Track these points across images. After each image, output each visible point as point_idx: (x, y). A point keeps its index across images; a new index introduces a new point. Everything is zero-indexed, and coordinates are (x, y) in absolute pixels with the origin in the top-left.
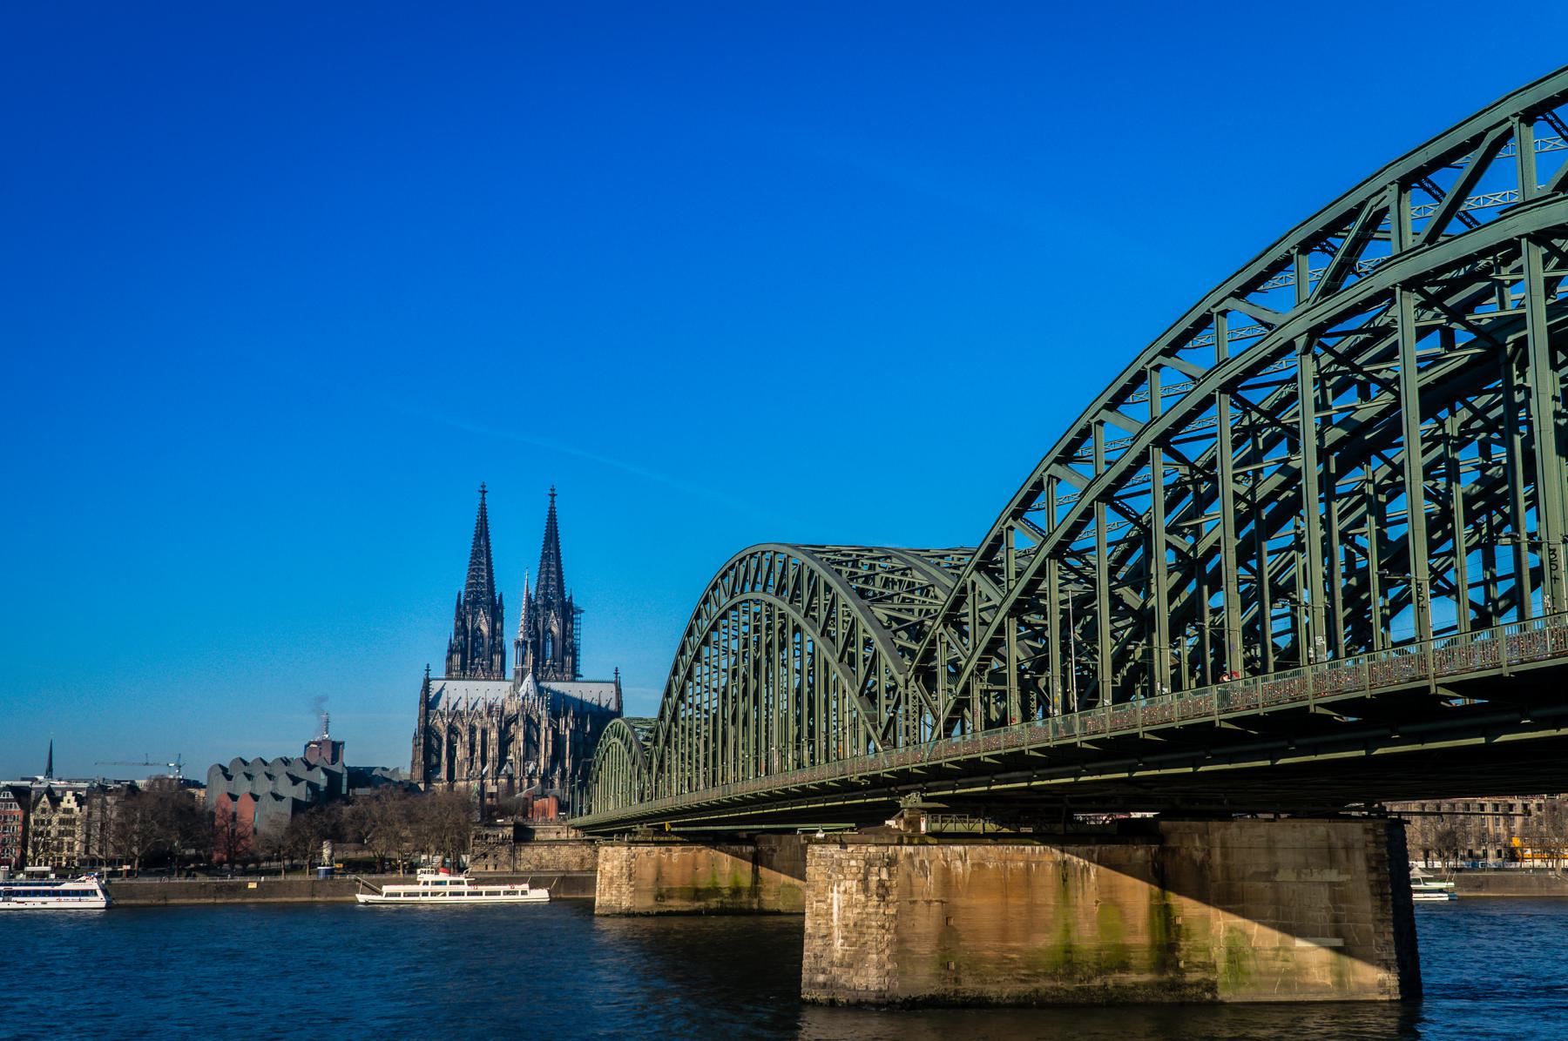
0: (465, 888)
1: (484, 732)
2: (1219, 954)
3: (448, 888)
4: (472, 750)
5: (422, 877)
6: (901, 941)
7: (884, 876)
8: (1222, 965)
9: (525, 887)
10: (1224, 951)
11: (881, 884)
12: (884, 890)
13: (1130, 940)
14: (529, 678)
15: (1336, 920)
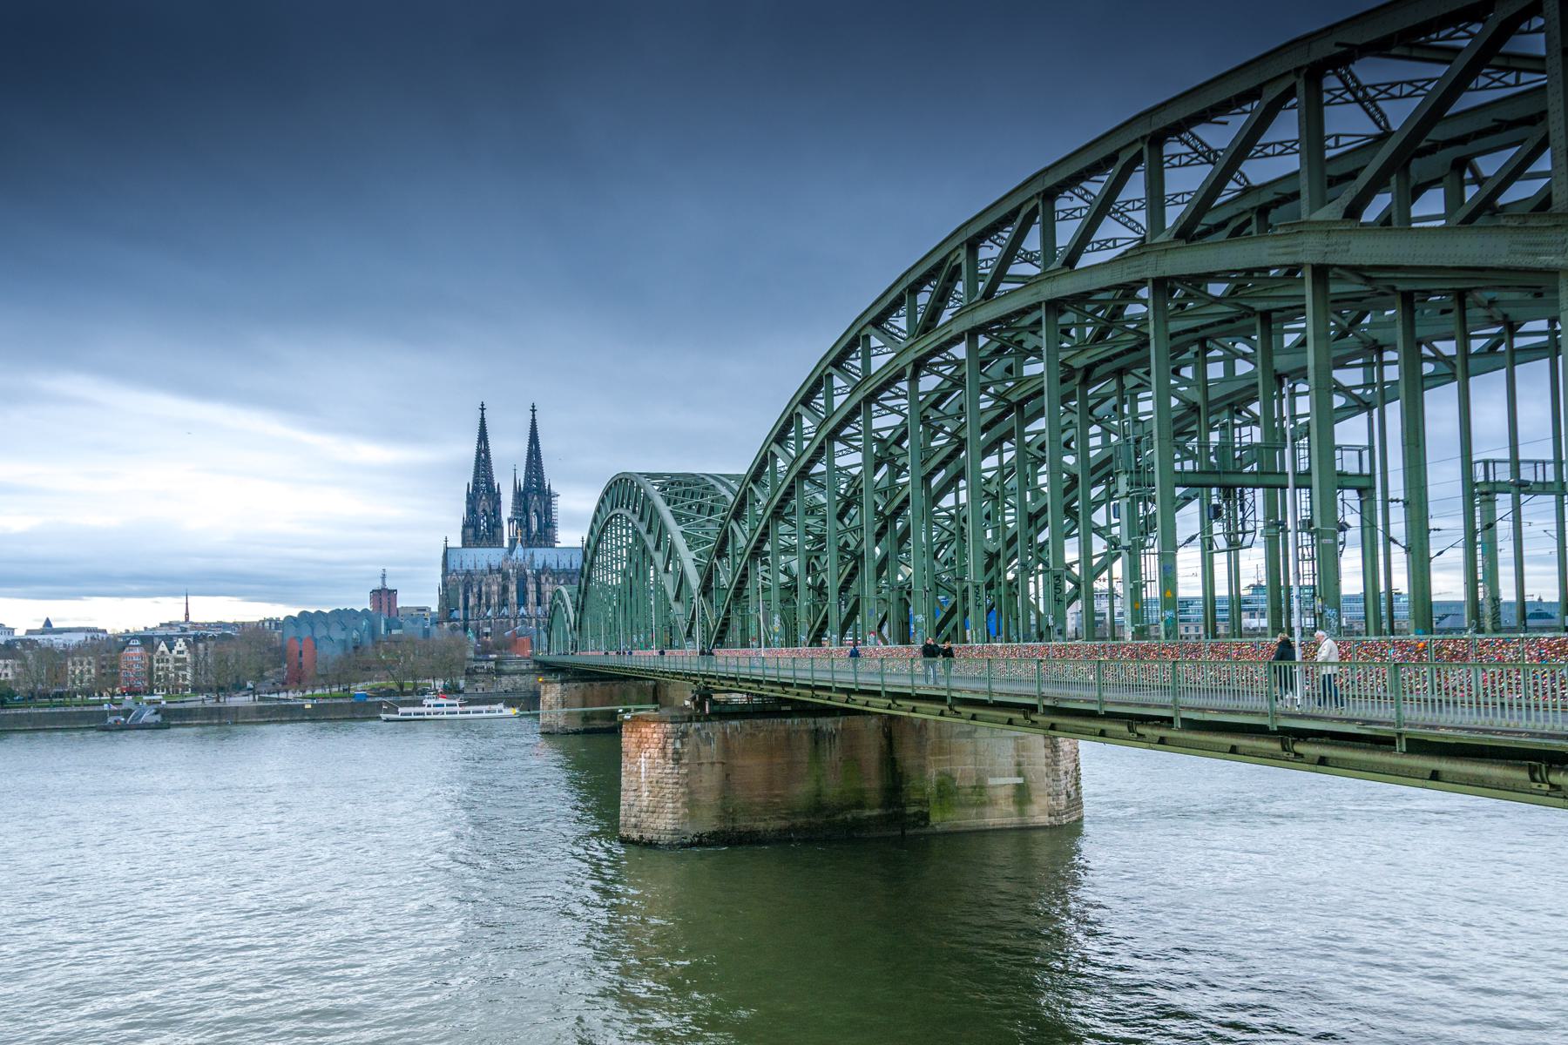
0: (458, 709)
1: (489, 585)
2: (931, 789)
3: (445, 709)
4: (480, 598)
5: (426, 701)
6: (691, 793)
7: (678, 745)
8: (932, 799)
9: (501, 706)
10: (935, 790)
11: (676, 752)
12: (677, 758)
13: (866, 785)
14: (519, 545)
15: (1019, 764)
